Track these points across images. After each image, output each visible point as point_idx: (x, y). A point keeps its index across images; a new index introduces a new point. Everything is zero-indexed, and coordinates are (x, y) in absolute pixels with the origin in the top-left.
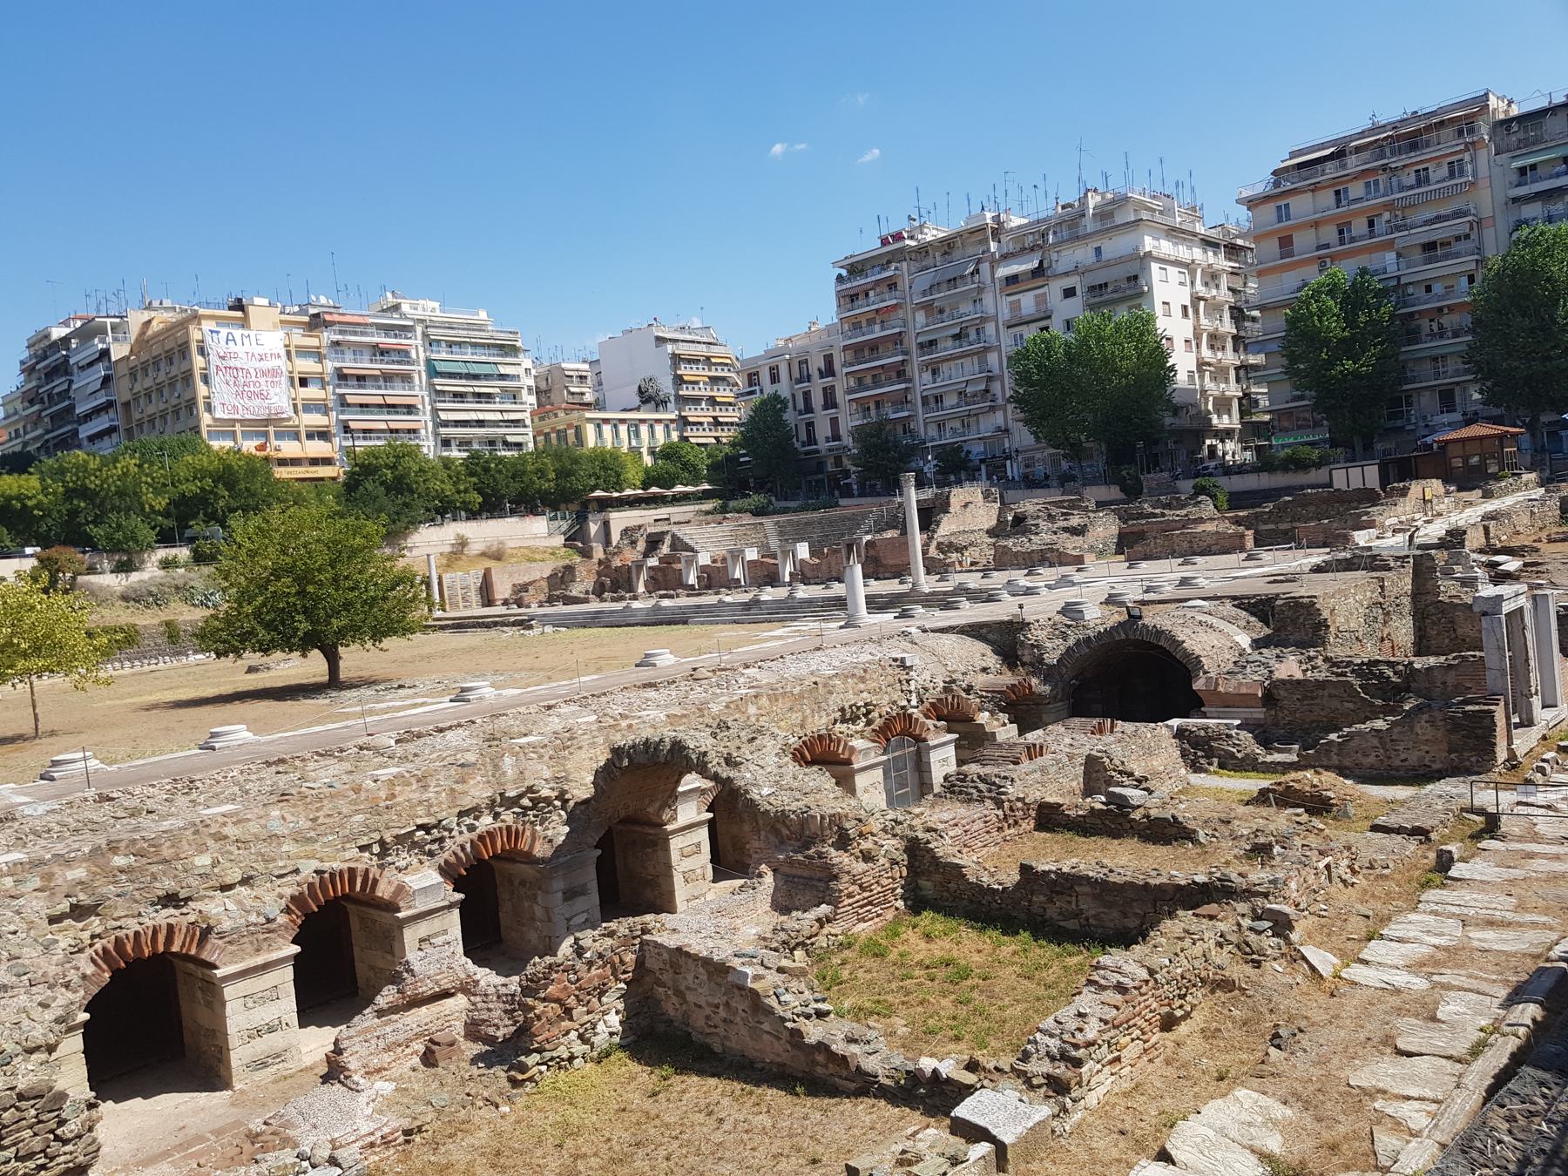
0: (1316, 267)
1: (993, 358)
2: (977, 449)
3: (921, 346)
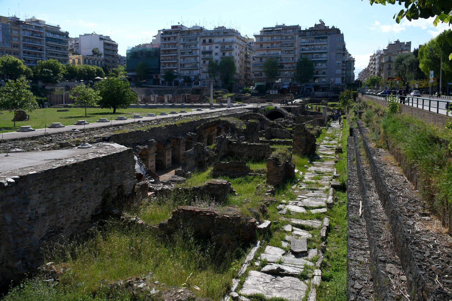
0: (266, 51)
1: (198, 58)
2: (193, 78)
3: (182, 53)
